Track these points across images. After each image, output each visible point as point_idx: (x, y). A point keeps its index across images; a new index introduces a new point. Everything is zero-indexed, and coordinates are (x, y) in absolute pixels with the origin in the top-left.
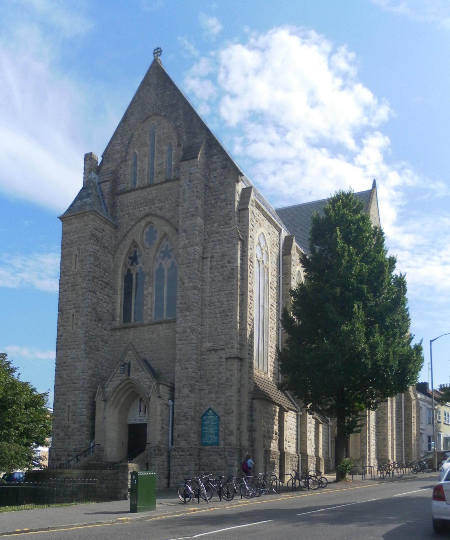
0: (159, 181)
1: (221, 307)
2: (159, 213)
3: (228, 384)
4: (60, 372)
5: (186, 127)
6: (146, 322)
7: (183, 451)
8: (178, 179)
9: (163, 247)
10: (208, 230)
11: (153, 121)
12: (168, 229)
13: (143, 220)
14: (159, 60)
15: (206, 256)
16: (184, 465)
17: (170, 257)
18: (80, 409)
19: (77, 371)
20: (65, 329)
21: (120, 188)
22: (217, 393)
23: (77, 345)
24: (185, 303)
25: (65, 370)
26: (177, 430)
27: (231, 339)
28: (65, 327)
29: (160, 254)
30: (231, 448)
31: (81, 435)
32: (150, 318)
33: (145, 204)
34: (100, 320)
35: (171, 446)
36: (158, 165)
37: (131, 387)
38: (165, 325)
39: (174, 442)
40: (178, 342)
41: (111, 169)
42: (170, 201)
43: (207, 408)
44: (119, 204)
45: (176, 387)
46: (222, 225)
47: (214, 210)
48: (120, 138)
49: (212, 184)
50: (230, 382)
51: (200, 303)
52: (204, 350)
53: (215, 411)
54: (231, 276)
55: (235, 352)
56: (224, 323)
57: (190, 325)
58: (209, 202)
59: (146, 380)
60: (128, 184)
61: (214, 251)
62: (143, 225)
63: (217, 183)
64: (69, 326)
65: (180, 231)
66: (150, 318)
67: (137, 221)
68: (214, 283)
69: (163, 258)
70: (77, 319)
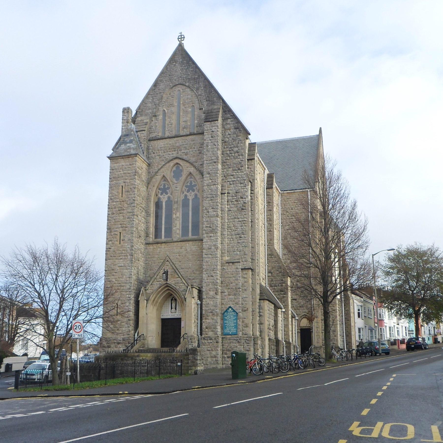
0: (184, 134)
1: (236, 231)
2: (185, 157)
3: (243, 288)
4: (109, 277)
5: (206, 96)
6: (175, 240)
7: (211, 339)
8: (202, 133)
9: (187, 183)
10: (224, 173)
11: (179, 89)
12: (192, 170)
13: (172, 162)
14: (183, 44)
15: (224, 192)
16: (212, 350)
17: (193, 191)
18: (127, 307)
19: (124, 277)
20: (113, 243)
21: (153, 135)
22: (235, 295)
23: (125, 256)
24: (210, 227)
25: (113, 275)
26: (205, 323)
27: (245, 255)
28: (113, 242)
29: (186, 188)
30: (247, 337)
31: (129, 327)
32: (178, 236)
33: (173, 149)
34: (140, 237)
35: (200, 336)
36: (184, 122)
37: (168, 289)
38: (191, 242)
39: (203, 333)
40: (204, 256)
41: (145, 121)
42: (194, 150)
43: (228, 306)
44: (151, 148)
45: (204, 289)
46: (235, 170)
47: (229, 158)
48: (152, 98)
49: (227, 139)
50: (245, 287)
51: (220, 227)
52: (224, 262)
53: (234, 309)
54: (244, 208)
55: (249, 265)
56: (239, 243)
57: (214, 243)
58: (225, 152)
59: (181, 284)
60: (158, 133)
61: (230, 189)
62: (171, 165)
63: (231, 139)
64: (117, 241)
65: (205, 173)
66: (178, 236)
67: (166, 162)
68: (230, 212)
69: (188, 191)
70: (124, 236)
